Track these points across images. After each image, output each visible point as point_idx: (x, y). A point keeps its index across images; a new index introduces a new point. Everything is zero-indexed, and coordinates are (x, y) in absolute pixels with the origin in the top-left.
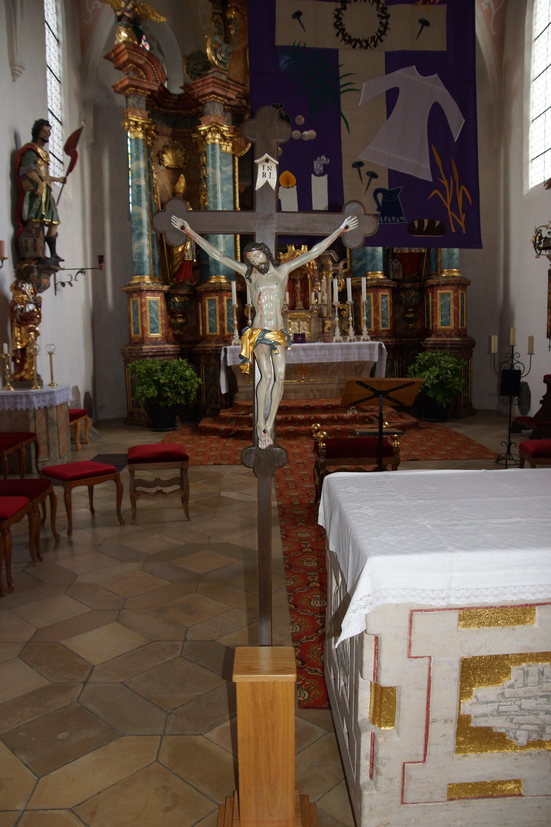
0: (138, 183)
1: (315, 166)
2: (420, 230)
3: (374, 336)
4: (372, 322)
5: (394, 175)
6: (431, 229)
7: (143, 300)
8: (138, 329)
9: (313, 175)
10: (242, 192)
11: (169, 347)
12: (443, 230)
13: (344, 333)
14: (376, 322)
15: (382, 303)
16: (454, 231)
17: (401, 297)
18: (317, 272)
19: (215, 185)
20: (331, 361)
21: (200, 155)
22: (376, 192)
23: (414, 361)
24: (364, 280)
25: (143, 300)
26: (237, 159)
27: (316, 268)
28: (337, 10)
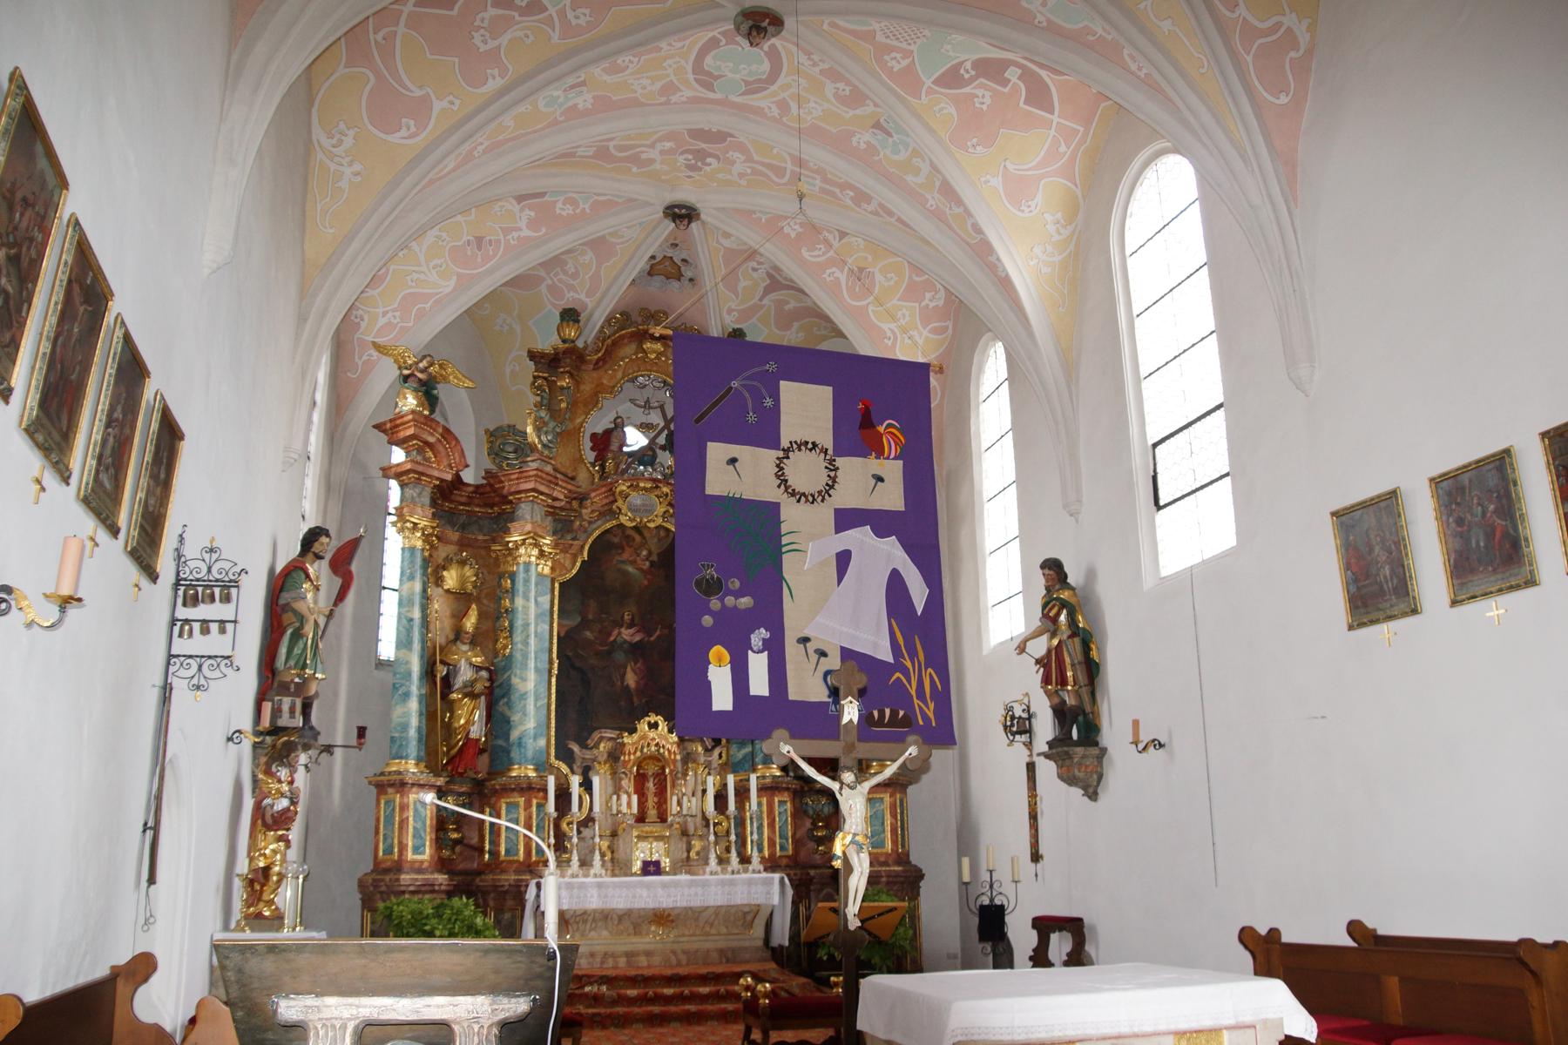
0: (409, 615)
1: (752, 641)
2: (880, 723)
3: (771, 865)
4: (766, 844)
5: (846, 654)
6: (894, 721)
7: (406, 800)
8: (392, 847)
9: (750, 652)
10: (562, 635)
11: (441, 878)
12: (908, 722)
13: (722, 861)
14: (772, 843)
15: (780, 813)
16: (921, 723)
17: (807, 804)
18: (679, 765)
19: (527, 625)
20: (706, 905)
21: (501, 576)
22: (827, 673)
24: (753, 778)
25: (406, 800)
26: (557, 585)
27: (678, 757)
28: (778, 458)
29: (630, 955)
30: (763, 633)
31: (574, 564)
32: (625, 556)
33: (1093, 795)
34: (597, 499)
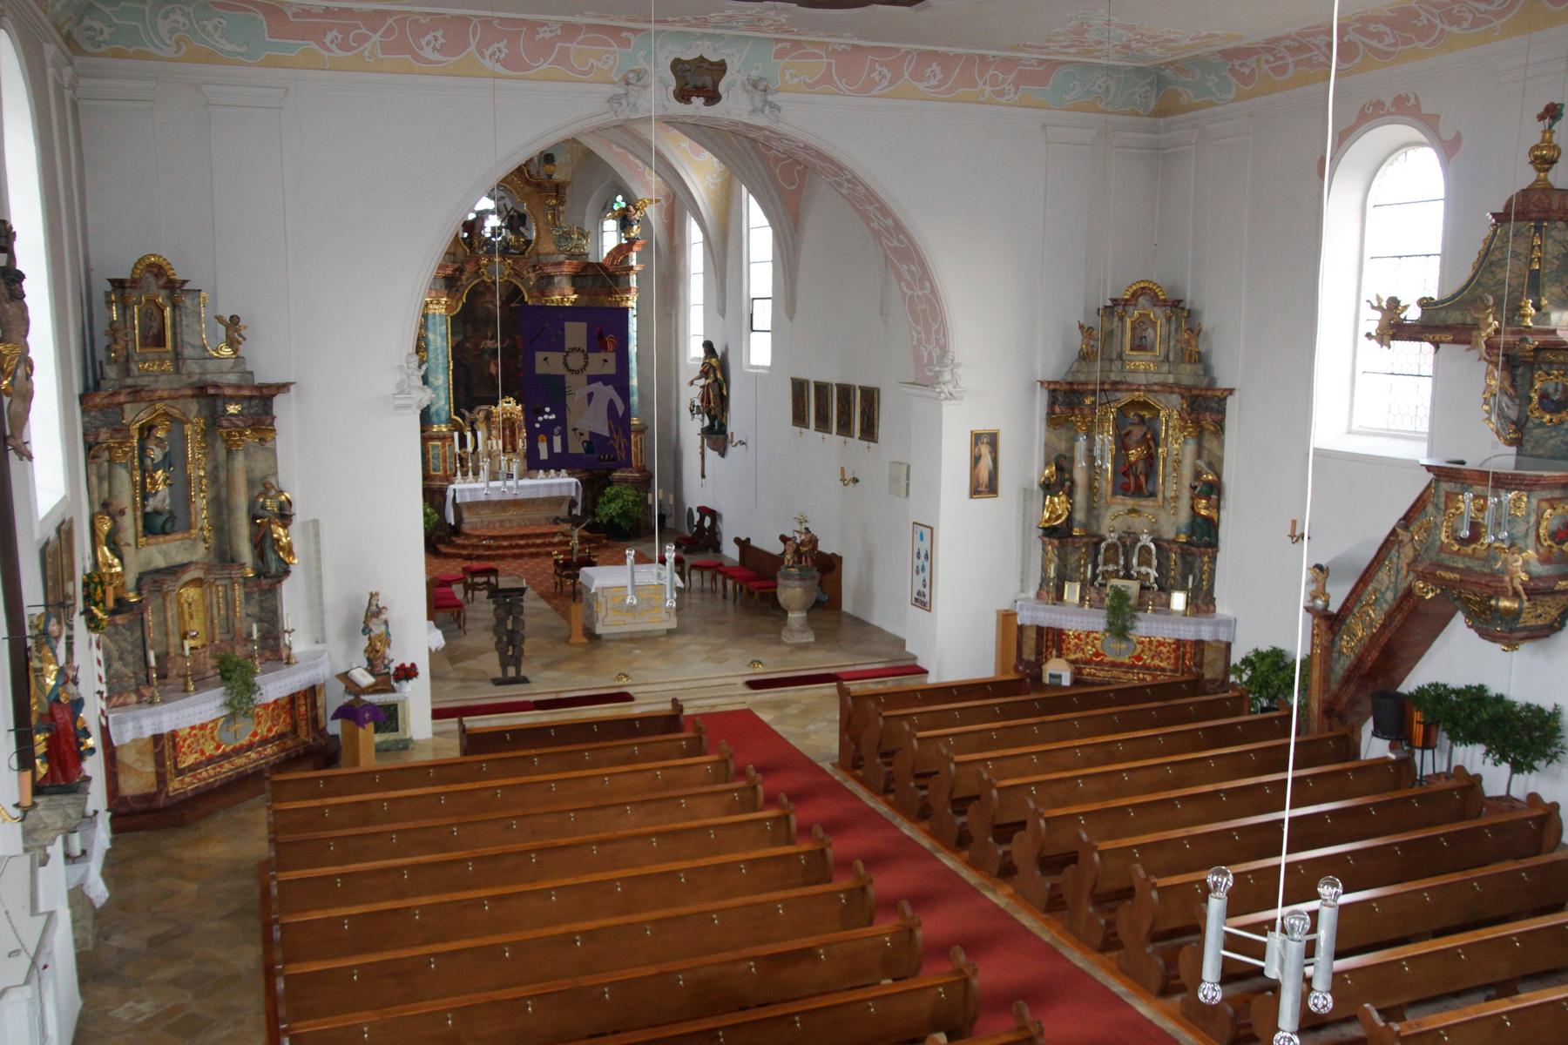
2: (604, 460)
5: (592, 434)
6: (609, 460)
12: (614, 459)
23: (604, 495)
26: (449, 318)
29: (501, 522)
30: (559, 428)
31: (457, 305)
32: (485, 300)
33: (723, 455)
34: (470, 268)
